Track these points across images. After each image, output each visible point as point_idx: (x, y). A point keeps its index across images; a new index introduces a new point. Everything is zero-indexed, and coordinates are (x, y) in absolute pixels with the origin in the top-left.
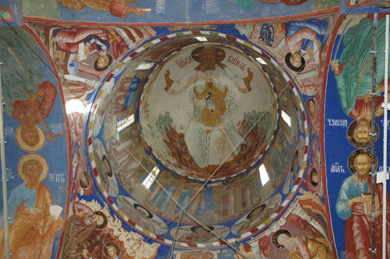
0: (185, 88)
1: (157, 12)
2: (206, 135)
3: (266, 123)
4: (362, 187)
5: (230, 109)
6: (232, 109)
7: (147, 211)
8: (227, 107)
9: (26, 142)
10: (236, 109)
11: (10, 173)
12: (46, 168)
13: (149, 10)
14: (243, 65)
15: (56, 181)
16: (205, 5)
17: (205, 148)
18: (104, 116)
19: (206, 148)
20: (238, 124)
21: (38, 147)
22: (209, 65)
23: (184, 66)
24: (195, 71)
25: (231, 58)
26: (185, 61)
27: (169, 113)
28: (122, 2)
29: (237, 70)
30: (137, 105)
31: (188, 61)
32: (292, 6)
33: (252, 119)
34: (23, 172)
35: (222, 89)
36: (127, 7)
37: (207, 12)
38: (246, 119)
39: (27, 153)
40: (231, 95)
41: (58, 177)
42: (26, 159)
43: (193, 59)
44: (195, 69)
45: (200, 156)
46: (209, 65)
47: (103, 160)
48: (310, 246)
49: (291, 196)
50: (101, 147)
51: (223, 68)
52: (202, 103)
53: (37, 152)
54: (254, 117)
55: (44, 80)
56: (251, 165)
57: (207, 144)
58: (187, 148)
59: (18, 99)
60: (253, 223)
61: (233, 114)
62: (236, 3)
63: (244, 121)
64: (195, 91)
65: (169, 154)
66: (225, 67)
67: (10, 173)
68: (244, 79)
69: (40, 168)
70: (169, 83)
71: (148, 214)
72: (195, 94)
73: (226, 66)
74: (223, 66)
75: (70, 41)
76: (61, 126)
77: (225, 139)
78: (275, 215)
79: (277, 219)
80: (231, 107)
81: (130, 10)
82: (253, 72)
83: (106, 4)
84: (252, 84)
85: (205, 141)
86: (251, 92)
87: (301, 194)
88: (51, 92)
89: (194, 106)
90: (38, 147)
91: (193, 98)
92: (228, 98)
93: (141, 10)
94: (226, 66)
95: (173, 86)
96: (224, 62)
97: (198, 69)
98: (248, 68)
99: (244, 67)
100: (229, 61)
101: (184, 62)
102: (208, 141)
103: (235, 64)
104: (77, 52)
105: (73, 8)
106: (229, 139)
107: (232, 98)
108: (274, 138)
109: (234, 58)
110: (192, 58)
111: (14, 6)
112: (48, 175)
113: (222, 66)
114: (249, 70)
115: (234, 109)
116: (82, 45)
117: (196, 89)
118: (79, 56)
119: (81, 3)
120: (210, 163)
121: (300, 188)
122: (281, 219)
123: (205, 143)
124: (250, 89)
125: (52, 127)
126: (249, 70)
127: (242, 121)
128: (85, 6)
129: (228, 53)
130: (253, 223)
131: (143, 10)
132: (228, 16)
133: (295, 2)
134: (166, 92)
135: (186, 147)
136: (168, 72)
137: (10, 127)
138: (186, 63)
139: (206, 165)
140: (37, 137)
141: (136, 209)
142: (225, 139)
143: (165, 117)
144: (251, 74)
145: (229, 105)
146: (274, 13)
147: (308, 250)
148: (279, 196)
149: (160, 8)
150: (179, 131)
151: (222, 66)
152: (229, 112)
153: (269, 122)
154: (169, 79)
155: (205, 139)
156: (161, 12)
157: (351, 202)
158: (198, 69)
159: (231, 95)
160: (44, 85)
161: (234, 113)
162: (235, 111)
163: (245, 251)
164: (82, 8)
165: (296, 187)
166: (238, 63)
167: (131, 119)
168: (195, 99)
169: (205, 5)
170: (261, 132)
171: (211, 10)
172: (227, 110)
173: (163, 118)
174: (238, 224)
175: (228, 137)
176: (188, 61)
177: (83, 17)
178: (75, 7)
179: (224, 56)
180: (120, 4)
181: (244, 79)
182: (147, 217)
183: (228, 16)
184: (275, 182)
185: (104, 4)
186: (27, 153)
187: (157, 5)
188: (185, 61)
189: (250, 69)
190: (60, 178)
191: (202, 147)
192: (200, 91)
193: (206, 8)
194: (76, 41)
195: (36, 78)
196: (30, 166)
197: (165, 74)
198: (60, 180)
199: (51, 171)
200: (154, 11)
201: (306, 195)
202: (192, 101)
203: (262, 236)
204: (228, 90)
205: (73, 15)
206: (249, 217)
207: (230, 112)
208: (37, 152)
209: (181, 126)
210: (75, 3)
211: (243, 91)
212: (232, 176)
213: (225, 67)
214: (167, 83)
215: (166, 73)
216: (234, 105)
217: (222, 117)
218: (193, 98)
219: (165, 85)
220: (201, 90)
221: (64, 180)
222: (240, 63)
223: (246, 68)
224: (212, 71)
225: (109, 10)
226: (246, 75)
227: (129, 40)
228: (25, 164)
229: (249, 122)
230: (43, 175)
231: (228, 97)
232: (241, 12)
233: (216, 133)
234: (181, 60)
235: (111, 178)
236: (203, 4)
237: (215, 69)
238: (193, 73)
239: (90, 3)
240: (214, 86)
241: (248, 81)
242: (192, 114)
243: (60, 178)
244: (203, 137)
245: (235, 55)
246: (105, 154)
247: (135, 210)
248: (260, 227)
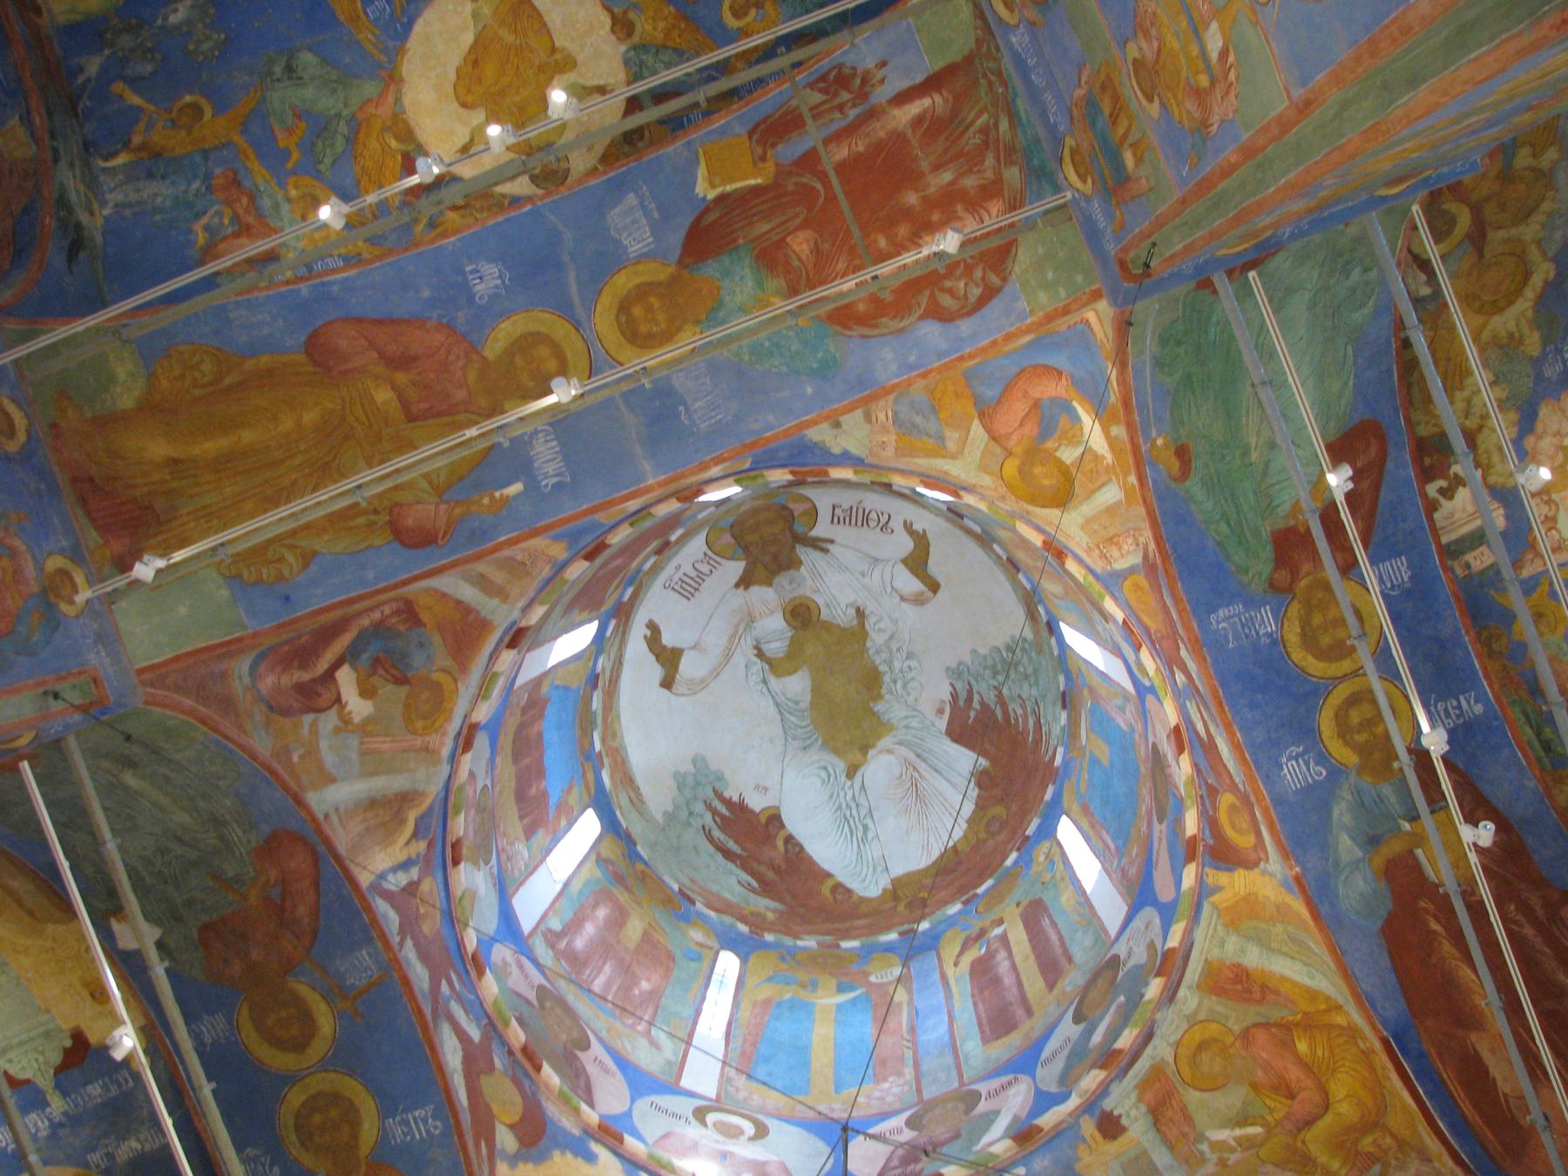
0: (728, 656)
1: (547, 485)
2: (849, 783)
3: (1026, 677)
4: (1393, 799)
5: (897, 670)
6: (901, 671)
7: (742, 1116)
8: (883, 668)
9: (279, 1044)
10: (914, 664)
11: (263, 1159)
12: (368, 1107)
13: (515, 488)
14: (884, 520)
15: (413, 1137)
16: (687, 409)
17: (861, 828)
18: (494, 861)
19: (866, 828)
20: (940, 711)
21: (319, 1048)
22: (775, 557)
23: (696, 590)
24: (741, 590)
25: (838, 511)
26: (693, 574)
27: (704, 759)
28: (425, 495)
29: (868, 538)
30: (590, 776)
31: (705, 568)
32: (958, 322)
33: (978, 676)
34: (302, 1144)
35: (843, 617)
36: (443, 507)
37: (702, 426)
38: (959, 685)
39: (292, 1079)
40: (882, 625)
41: (416, 1123)
42: (295, 1098)
43: (718, 559)
44: (737, 585)
45: (854, 859)
46: (775, 557)
47: (542, 1007)
48: (1302, 1047)
49: (1185, 907)
50: (521, 967)
51: (826, 551)
52: (797, 685)
53: (324, 1065)
54: (981, 670)
55: (266, 829)
56: (1029, 832)
57: (863, 812)
58: (802, 848)
59: (205, 918)
60: (1097, 1038)
61: (914, 684)
62: (784, 369)
63: (955, 696)
64: (760, 654)
65: (754, 891)
66: (830, 546)
67: (263, 1159)
68: (905, 561)
69: (351, 1115)
70: (669, 659)
71: (749, 1128)
72: (766, 667)
73: (832, 542)
74: (824, 545)
75: (306, 676)
76: (369, 954)
77: (916, 775)
78: (1154, 987)
79: (1170, 995)
80: (897, 665)
81: (458, 511)
82: (924, 531)
83: (374, 523)
84: (934, 567)
85: (853, 806)
86: (940, 593)
87: (1217, 889)
88: (298, 861)
89: (777, 705)
90: (319, 1048)
91: (765, 681)
92: (876, 639)
93: (492, 497)
94: (832, 542)
95: (689, 667)
96: (821, 530)
97: (745, 582)
98: (905, 522)
99: (890, 524)
100: (836, 519)
101: (692, 578)
102: (863, 801)
103: (859, 523)
104: (338, 700)
105: (281, 578)
106: (929, 769)
107: (889, 633)
108: (1069, 718)
109: (846, 506)
110: (713, 556)
111: (98, 653)
112: (384, 1127)
113: (819, 545)
114: (908, 527)
115: (910, 668)
116: (346, 678)
117: (765, 647)
118: (347, 710)
119: (299, 551)
120: (898, 870)
121: (1207, 869)
122: (1182, 992)
123: (854, 812)
124: (934, 587)
125: (342, 969)
126: (908, 527)
127: (948, 697)
128: (315, 554)
129: (823, 500)
130: (1097, 1038)
131: (497, 494)
132: (771, 418)
133: (963, 307)
134: (665, 691)
135: (797, 850)
136: (654, 628)
137: (211, 1013)
138: (701, 577)
139: (884, 882)
140: (307, 1019)
141: (704, 1124)
142: (916, 775)
143: (694, 775)
144: (921, 542)
145: (889, 663)
146: (912, 359)
147: (1300, 1061)
148: (1149, 914)
149: (550, 468)
150: (756, 803)
151: (819, 545)
152: (895, 682)
153: (1035, 671)
154: (664, 648)
155: (849, 797)
156: (555, 480)
157: (1379, 861)
158: (745, 582)
159: (882, 625)
160: (271, 847)
161: (913, 679)
162: (913, 674)
163: (1104, 1138)
164: (306, 566)
165: (1189, 875)
166: (866, 519)
167: (588, 826)
168: (772, 680)
169: (687, 409)
170: (1020, 712)
171: (711, 417)
172: (887, 678)
173: (690, 780)
174: (1054, 1055)
175: (923, 765)
176: (705, 568)
177: (319, 591)
178: (286, 572)
179: (813, 513)
180: (420, 507)
181: (905, 561)
182: (751, 1139)
183: (771, 418)
184: (1123, 870)
185: (371, 524)
186: (291, 1079)
187: (536, 465)
188: (693, 574)
189: (911, 524)
190: (425, 1121)
191: (850, 826)
192: (776, 648)
193: (695, 417)
194: (323, 665)
195: (241, 834)
196: (317, 1118)
197: (645, 637)
198: (428, 1131)
199: (386, 1111)
200: (532, 486)
201: (1236, 883)
202: (765, 689)
203: (1142, 1065)
204: (867, 612)
205: (287, 598)
206: (1077, 1019)
207: (899, 684)
208: (324, 1065)
209: (757, 787)
210: (281, 560)
211: (918, 600)
212: (980, 890)
213: (830, 546)
214: (663, 665)
215: (648, 633)
216: (904, 655)
217: (879, 707)
218: (765, 681)
219: (657, 672)
220: (778, 644)
221: (439, 1123)
222: (873, 516)
223: (897, 524)
224: (792, 572)
225: (392, 537)
226: (908, 544)
227: (487, 599)
228: (298, 1115)
229: (970, 692)
230: (369, 1132)
231: (873, 634)
232: (809, 390)
233: (880, 768)
234: (680, 574)
235: (589, 1053)
236: (681, 408)
237: (801, 563)
238: (739, 598)
239: (326, 538)
240: (815, 619)
241: (917, 562)
242: (777, 730)
243: (425, 1121)
244: (842, 794)
245: (847, 499)
246: (538, 979)
247: (703, 1131)
248: (1126, 1040)
